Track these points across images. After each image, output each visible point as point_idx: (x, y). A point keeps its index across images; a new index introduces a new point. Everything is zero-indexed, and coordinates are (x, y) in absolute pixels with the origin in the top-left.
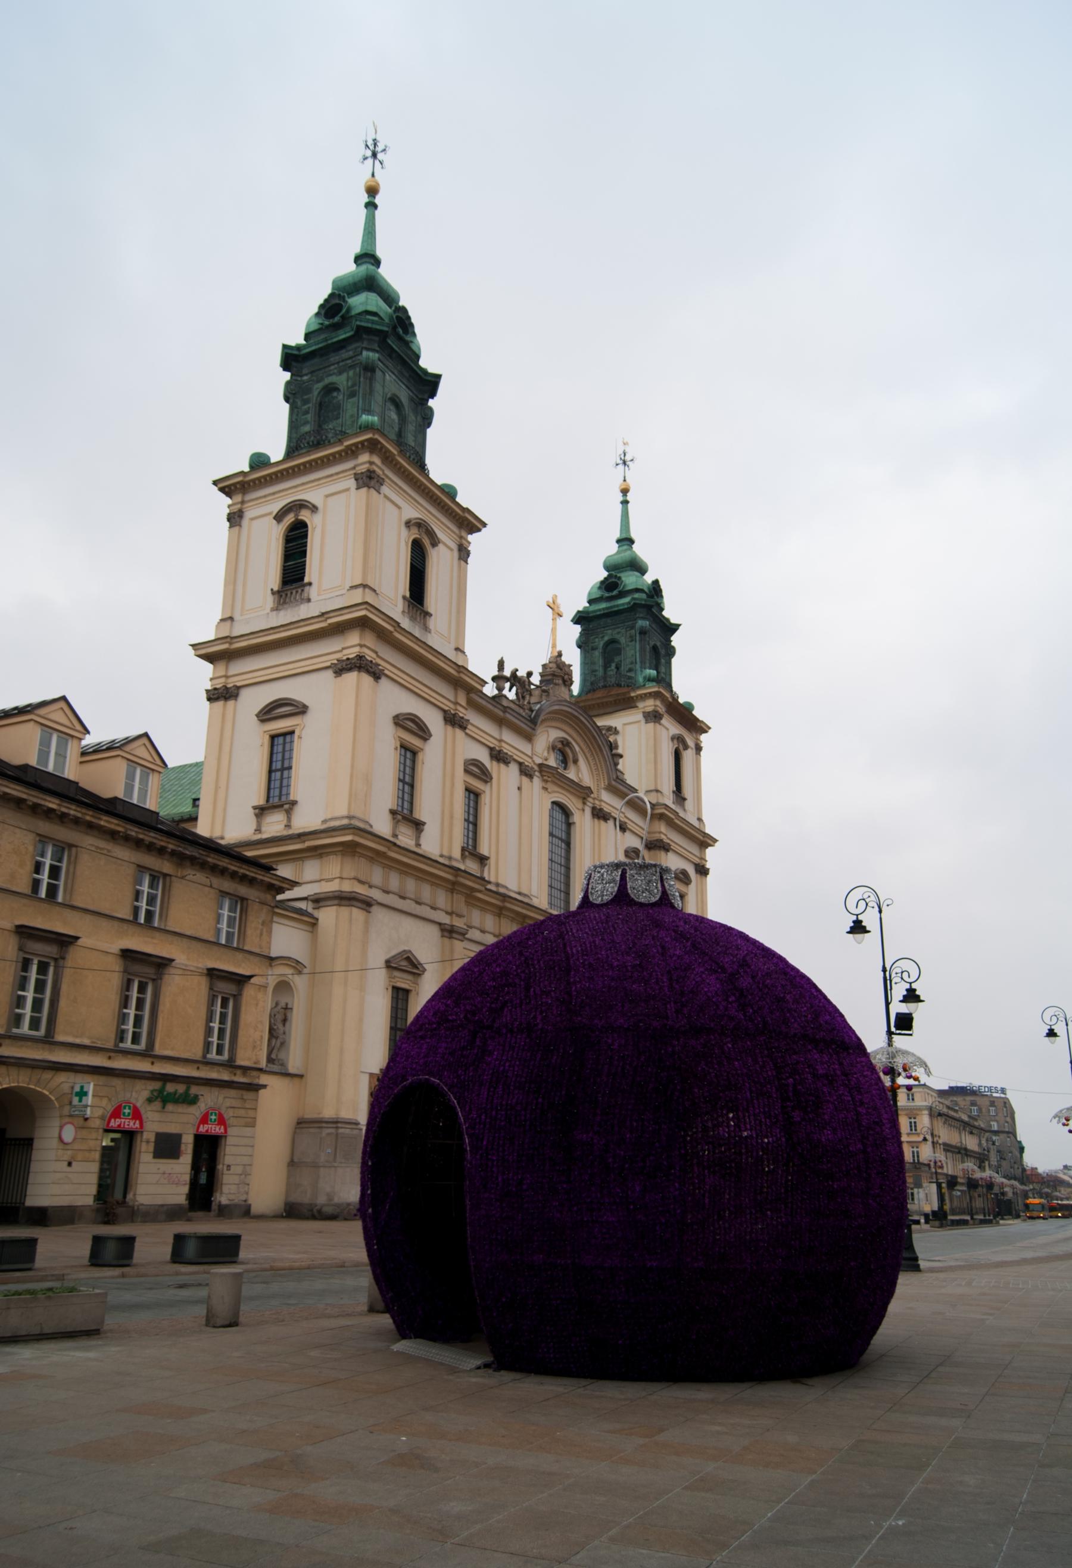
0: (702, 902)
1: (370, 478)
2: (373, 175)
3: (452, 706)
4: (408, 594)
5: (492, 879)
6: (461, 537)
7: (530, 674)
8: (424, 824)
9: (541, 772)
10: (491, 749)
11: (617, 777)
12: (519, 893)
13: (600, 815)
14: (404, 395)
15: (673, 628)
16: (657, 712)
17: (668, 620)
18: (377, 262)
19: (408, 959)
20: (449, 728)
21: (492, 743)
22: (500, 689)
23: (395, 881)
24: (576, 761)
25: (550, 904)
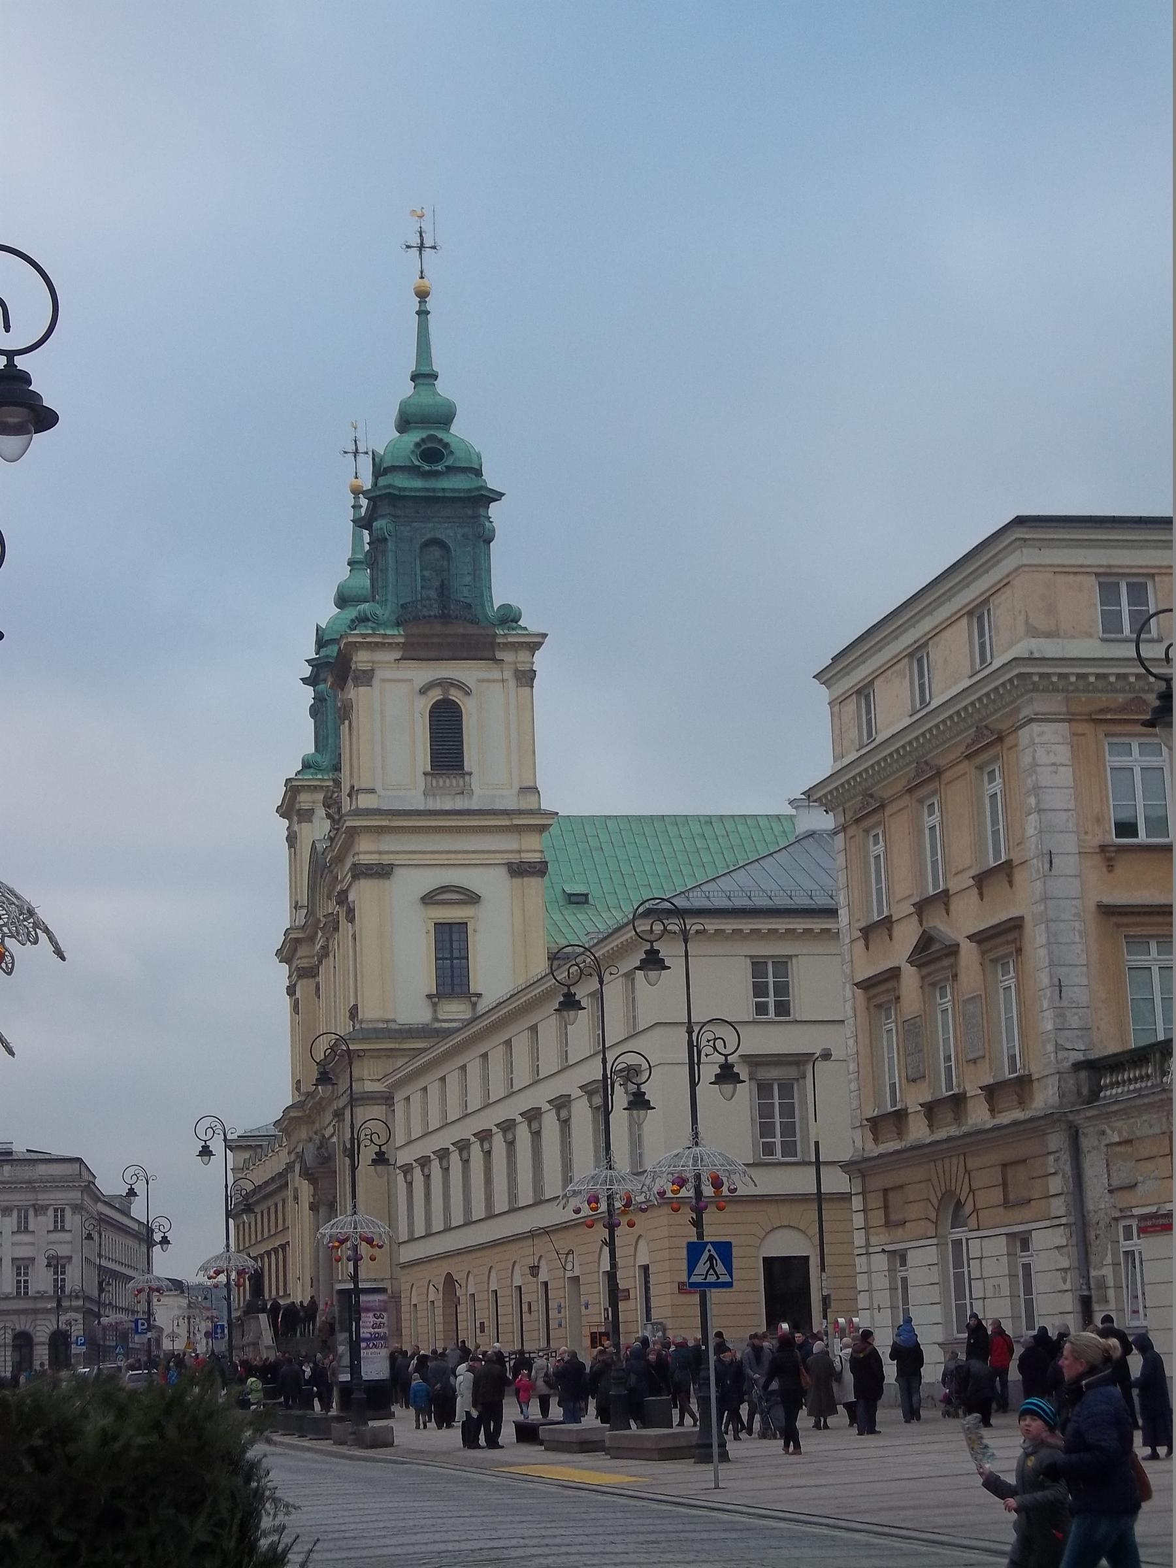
2: (422, 277)
20: (517, 881)
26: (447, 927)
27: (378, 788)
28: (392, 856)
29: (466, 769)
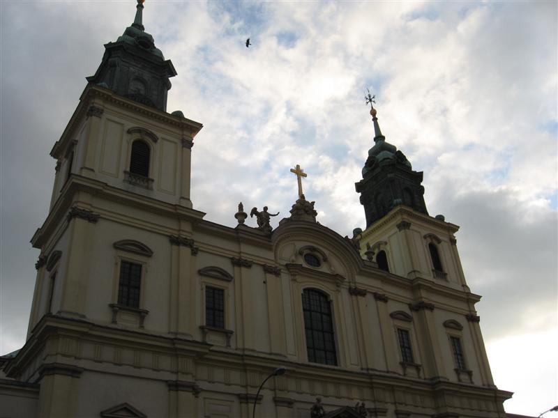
0: (477, 340)
1: (92, 111)
3: (176, 232)
4: (128, 170)
5: (240, 346)
6: (183, 135)
7: (266, 208)
8: (147, 312)
9: (288, 270)
10: (232, 259)
11: (365, 265)
12: (271, 354)
13: (356, 292)
14: (147, 76)
15: (420, 176)
16: (404, 222)
17: (415, 172)
18: (142, 28)
19: (125, 409)
20: (175, 247)
21: (231, 255)
22: (241, 222)
23: (108, 353)
24: (325, 260)
25: (310, 360)
26: (128, 266)
27: (96, 171)
28: (100, 211)
29: (150, 177)
